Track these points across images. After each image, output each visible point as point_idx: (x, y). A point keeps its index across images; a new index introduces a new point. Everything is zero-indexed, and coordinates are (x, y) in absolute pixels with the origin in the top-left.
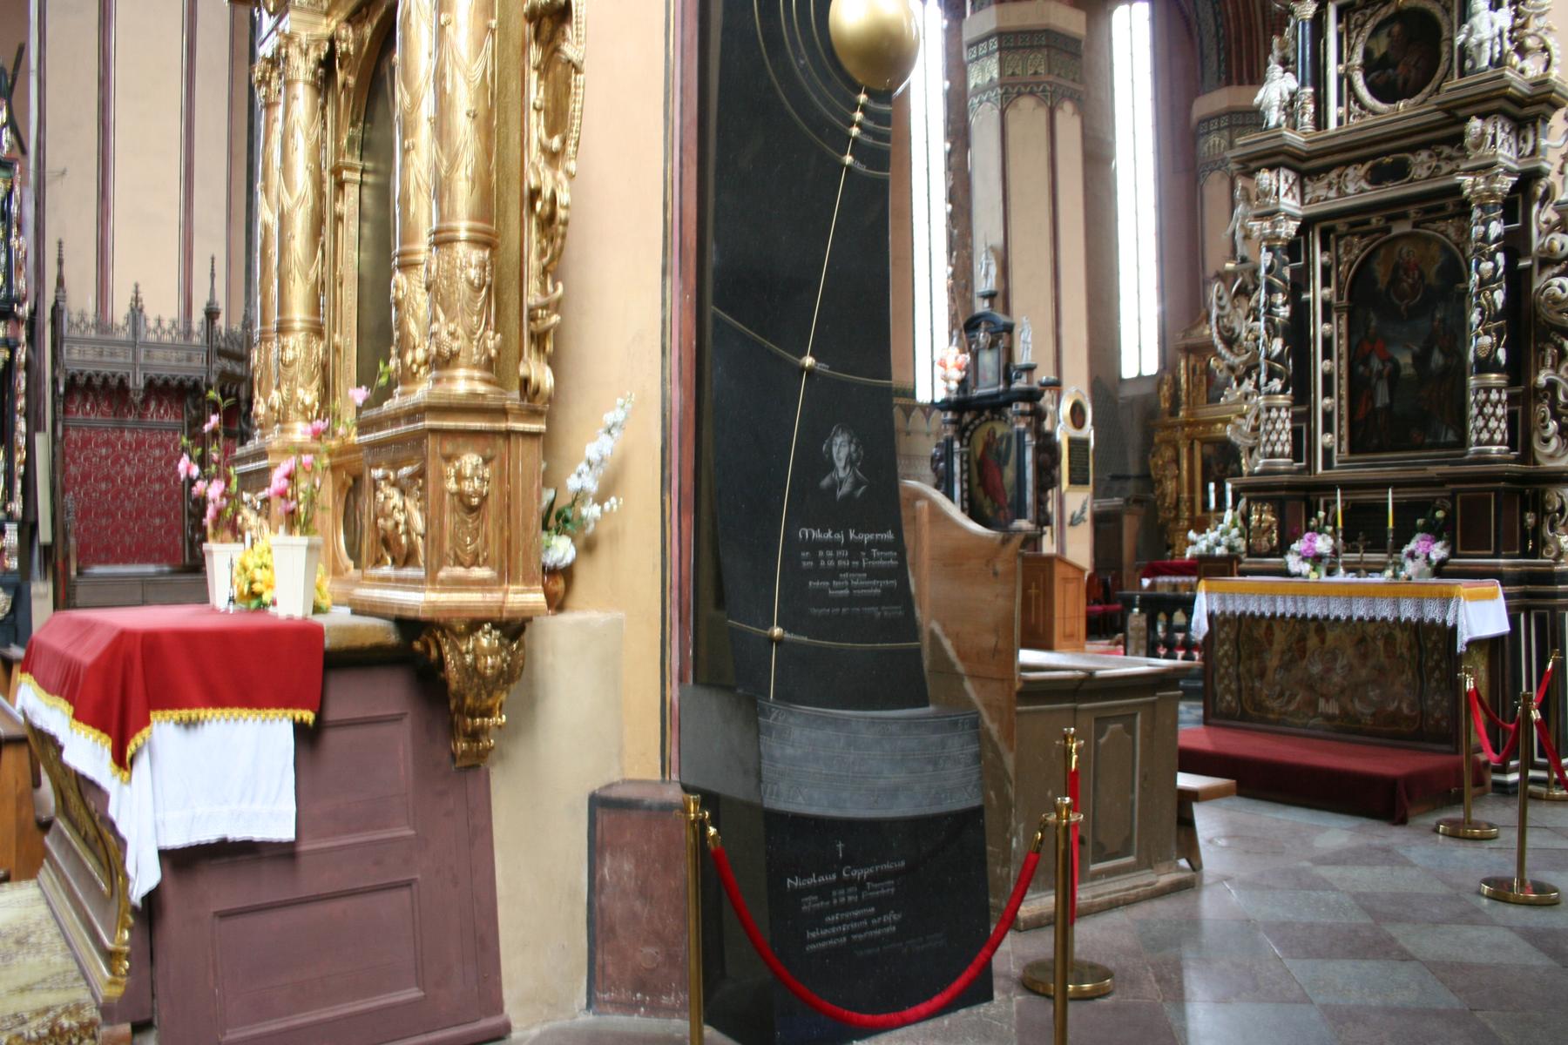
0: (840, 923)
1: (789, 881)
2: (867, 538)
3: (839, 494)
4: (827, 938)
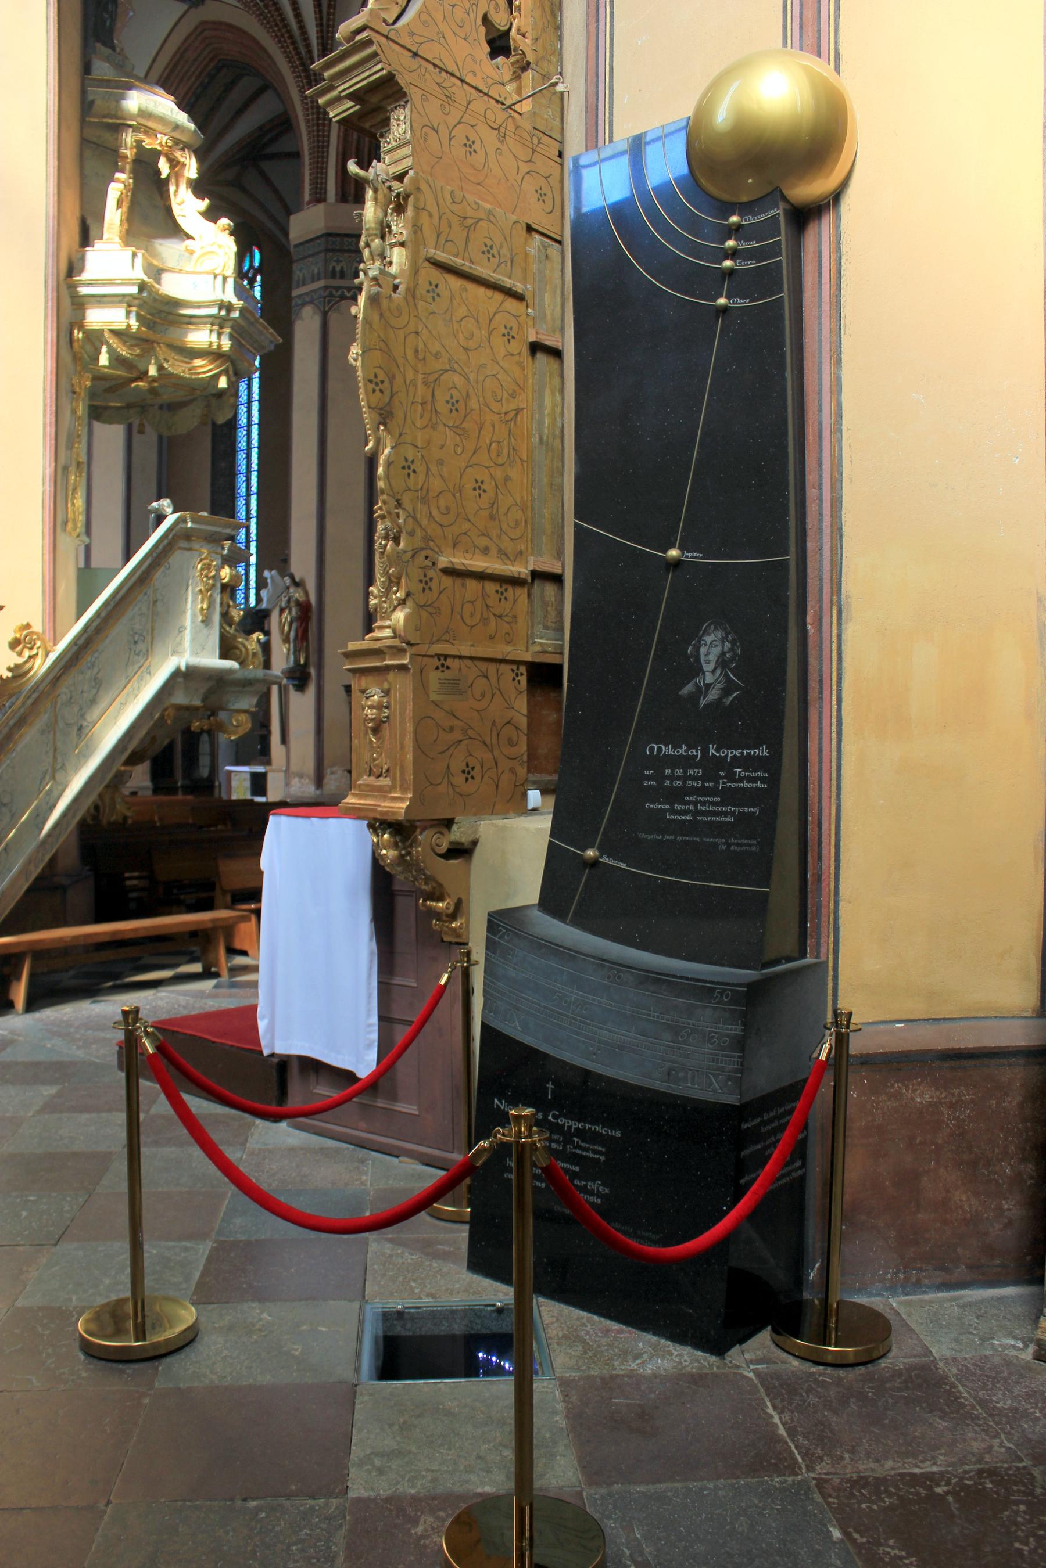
2: (730, 754)
3: (703, 702)
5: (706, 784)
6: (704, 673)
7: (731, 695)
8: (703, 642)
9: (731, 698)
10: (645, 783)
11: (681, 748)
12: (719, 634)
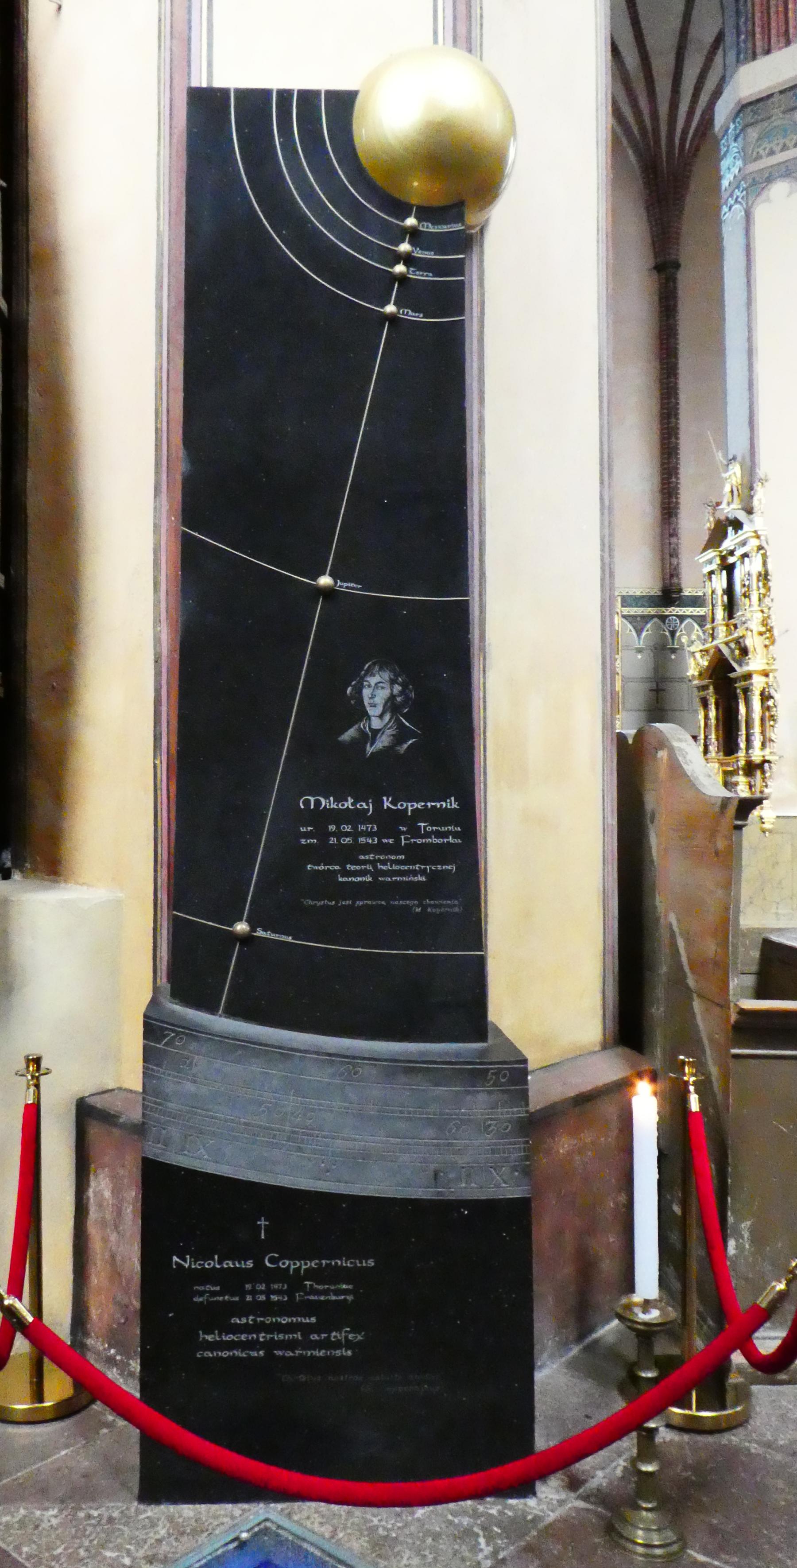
0: (257, 1328)
1: (175, 1259)
3: (370, 750)
4: (231, 1345)
5: (385, 841)
6: (369, 718)
7: (406, 742)
8: (365, 683)
9: (405, 746)
10: (303, 841)
11: (347, 801)
12: (386, 675)
